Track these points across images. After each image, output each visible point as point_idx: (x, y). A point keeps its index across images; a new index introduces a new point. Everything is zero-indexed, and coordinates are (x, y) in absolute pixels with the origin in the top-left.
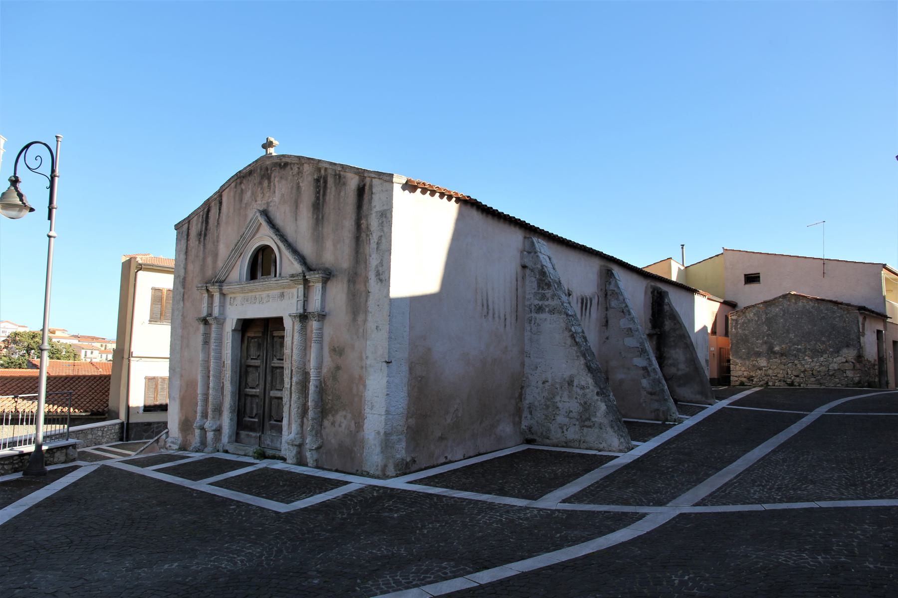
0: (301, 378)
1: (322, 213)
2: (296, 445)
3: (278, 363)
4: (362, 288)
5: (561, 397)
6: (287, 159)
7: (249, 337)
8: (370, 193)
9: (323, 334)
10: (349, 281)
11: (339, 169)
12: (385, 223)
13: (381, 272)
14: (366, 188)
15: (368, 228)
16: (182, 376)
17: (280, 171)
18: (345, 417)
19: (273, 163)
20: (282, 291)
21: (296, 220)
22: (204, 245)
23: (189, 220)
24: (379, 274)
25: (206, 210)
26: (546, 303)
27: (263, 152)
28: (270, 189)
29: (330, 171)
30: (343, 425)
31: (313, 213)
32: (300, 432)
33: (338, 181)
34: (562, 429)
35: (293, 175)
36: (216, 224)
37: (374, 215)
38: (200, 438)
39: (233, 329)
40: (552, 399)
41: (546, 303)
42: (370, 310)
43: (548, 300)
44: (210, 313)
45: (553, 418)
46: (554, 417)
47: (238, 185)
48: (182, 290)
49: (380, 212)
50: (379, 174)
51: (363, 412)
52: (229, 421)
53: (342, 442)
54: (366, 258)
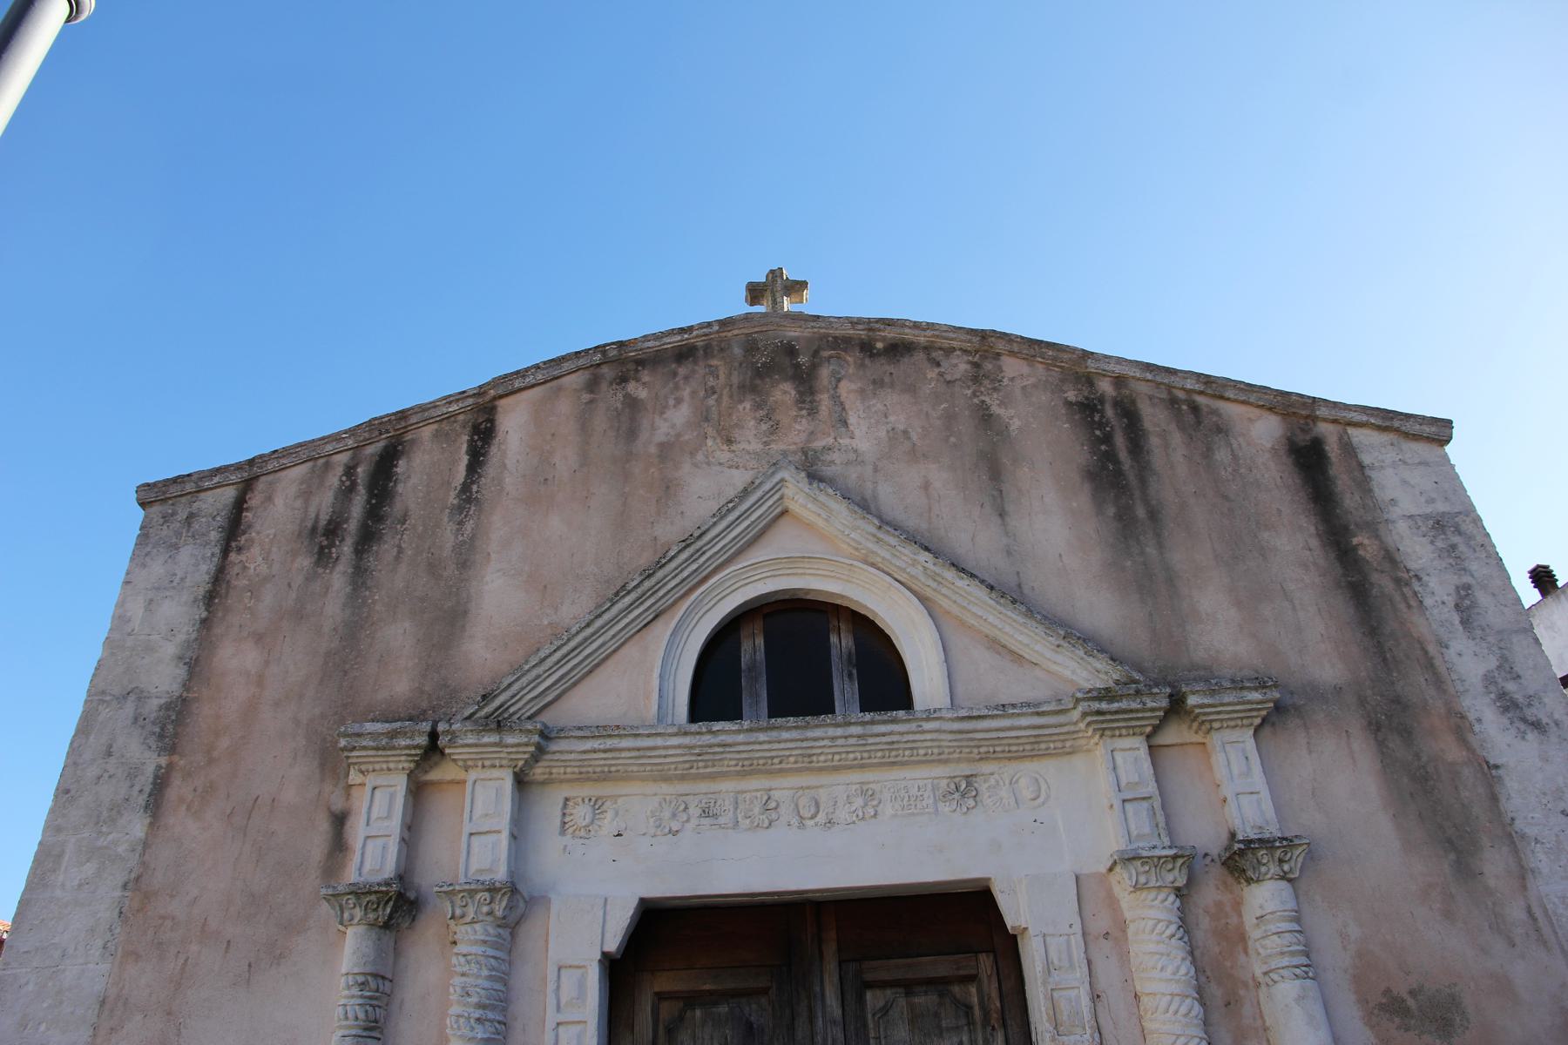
1: (1146, 501)
6: (907, 331)
7: (660, 997)
12: (1462, 548)
13: (1519, 697)
17: (867, 361)
19: (828, 335)
20: (966, 769)
21: (1002, 514)
22: (360, 575)
25: (373, 450)
28: (813, 412)
31: (1099, 505)
33: (1190, 418)
36: (452, 499)
37: (1402, 527)
39: (613, 945)
47: (604, 386)
48: (151, 761)
49: (1426, 517)
50: (1389, 422)
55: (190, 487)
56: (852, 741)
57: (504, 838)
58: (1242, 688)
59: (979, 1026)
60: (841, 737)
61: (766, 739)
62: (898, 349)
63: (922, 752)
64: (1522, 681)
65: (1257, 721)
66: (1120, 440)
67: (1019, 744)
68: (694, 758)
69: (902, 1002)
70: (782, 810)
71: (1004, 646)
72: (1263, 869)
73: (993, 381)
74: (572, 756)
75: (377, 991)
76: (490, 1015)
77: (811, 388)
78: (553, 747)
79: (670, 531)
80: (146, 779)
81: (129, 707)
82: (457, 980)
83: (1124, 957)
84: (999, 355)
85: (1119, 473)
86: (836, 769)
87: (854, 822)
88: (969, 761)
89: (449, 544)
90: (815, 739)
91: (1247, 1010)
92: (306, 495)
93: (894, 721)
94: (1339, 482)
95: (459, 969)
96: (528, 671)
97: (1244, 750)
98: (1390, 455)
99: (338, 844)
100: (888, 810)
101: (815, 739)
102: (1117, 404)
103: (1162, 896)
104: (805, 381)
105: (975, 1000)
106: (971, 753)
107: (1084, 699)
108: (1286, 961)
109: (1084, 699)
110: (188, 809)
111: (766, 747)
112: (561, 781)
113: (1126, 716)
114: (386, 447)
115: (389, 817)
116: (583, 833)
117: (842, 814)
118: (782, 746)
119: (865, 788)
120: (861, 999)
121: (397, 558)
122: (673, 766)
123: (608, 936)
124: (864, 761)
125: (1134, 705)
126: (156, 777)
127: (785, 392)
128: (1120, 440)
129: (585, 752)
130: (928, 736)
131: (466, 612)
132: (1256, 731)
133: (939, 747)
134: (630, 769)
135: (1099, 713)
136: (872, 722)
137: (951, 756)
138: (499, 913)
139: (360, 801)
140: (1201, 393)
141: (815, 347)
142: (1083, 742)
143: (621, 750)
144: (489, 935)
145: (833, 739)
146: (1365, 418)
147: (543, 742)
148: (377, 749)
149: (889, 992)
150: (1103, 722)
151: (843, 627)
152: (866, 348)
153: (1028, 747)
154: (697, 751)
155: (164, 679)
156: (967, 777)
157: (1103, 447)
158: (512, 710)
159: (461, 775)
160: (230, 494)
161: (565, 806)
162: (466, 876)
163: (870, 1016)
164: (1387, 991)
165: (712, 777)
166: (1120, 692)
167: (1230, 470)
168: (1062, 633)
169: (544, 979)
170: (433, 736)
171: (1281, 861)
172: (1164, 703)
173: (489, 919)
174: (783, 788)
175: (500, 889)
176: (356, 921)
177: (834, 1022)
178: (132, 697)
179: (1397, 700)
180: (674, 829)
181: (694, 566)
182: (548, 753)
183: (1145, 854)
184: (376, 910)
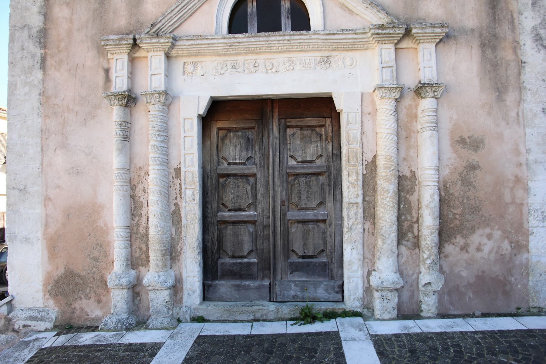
2: (397, 290)
3: (303, 168)
4: (509, 55)
7: (219, 129)
10: (483, 45)
16: (47, 199)
18: (489, 237)
20: (327, 54)
24: (541, 39)
30: (486, 249)
38: (127, 304)
42: (528, 87)
44: (130, 88)
48: (39, 52)
51: (525, 226)
53: (483, 272)
54: (512, 16)
56: (286, 42)
57: (163, 76)
58: (434, 27)
59: (324, 141)
60: (282, 40)
61: (254, 40)
63: (311, 47)
65: (438, 40)
67: (347, 45)
68: (228, 47)
69: (299, 132)
70: (260, 67)
71: (346, 7)
72: (427, 94)
74: (185, 47)
75: (126, 126)
76: (162, 134)
78: (178, 43)
82: (151, 123)
83: (374, 121)
86: (280, 52)
87: (285, 72)
88: (329, 51)
90: (272, 41)
91: (413, 140)
93: (301, 35)
95: (151, 119)
96: (167, 15)
99: (108, 80)
100: (298, 67)
101: (272, 41)
103: (390, 101)
105: (323, 133)
106: (329, 47)
107: (373, 28)
108: (429, 125)
109: (373, 28)
110: (55, 68)
111: (254, 43)
112: (182, 56)
113: (388, 36)
115: (123, 69)
116: (191, 75)
117: (281, 68)
118: (260, 43)
119: (290, 59)
120: (285, 131)
122: (221, 50)
123: (200, 109)
124: (290, 50)
125: (392, 32)
126: (42, 57)
129: (189, 45)
130: (314, 41)
132: (437, 44)
133: (318, 45)
134: (206, 51)
135: (378, 34)
136: (293, 35)
137: (322, 49)
138: (162, 101)
139: (113, 64)
142: (371, 45)
143: (202, 44)
144: (160, 108)
145: (279, 41)
148: (115, 45)
149: (295, 129)
150: (379, 38)
153: (350, 46)
154: (229, 45)
156: (327, 56)
158: (163, 30)
159: (147, 54)
161: (184, 65)
162: (151, 88)
163: (288, 136)
164: (461, 136)
165: (236, 55)
166: (387, 26)
168: (369, 2)
169: (179, 123)
170: (135, 40)
171: (434, 91)
172: (403, 31)
173: (159, 103)
174: (261, 59)
175: (162, 93)
176: (116, 104)
177: (276, 138)
178: (26, 28)
179: (494, 35)
180: (222, 73)
182: (176, 46)
183: (386, 86)
184: (121, 101)
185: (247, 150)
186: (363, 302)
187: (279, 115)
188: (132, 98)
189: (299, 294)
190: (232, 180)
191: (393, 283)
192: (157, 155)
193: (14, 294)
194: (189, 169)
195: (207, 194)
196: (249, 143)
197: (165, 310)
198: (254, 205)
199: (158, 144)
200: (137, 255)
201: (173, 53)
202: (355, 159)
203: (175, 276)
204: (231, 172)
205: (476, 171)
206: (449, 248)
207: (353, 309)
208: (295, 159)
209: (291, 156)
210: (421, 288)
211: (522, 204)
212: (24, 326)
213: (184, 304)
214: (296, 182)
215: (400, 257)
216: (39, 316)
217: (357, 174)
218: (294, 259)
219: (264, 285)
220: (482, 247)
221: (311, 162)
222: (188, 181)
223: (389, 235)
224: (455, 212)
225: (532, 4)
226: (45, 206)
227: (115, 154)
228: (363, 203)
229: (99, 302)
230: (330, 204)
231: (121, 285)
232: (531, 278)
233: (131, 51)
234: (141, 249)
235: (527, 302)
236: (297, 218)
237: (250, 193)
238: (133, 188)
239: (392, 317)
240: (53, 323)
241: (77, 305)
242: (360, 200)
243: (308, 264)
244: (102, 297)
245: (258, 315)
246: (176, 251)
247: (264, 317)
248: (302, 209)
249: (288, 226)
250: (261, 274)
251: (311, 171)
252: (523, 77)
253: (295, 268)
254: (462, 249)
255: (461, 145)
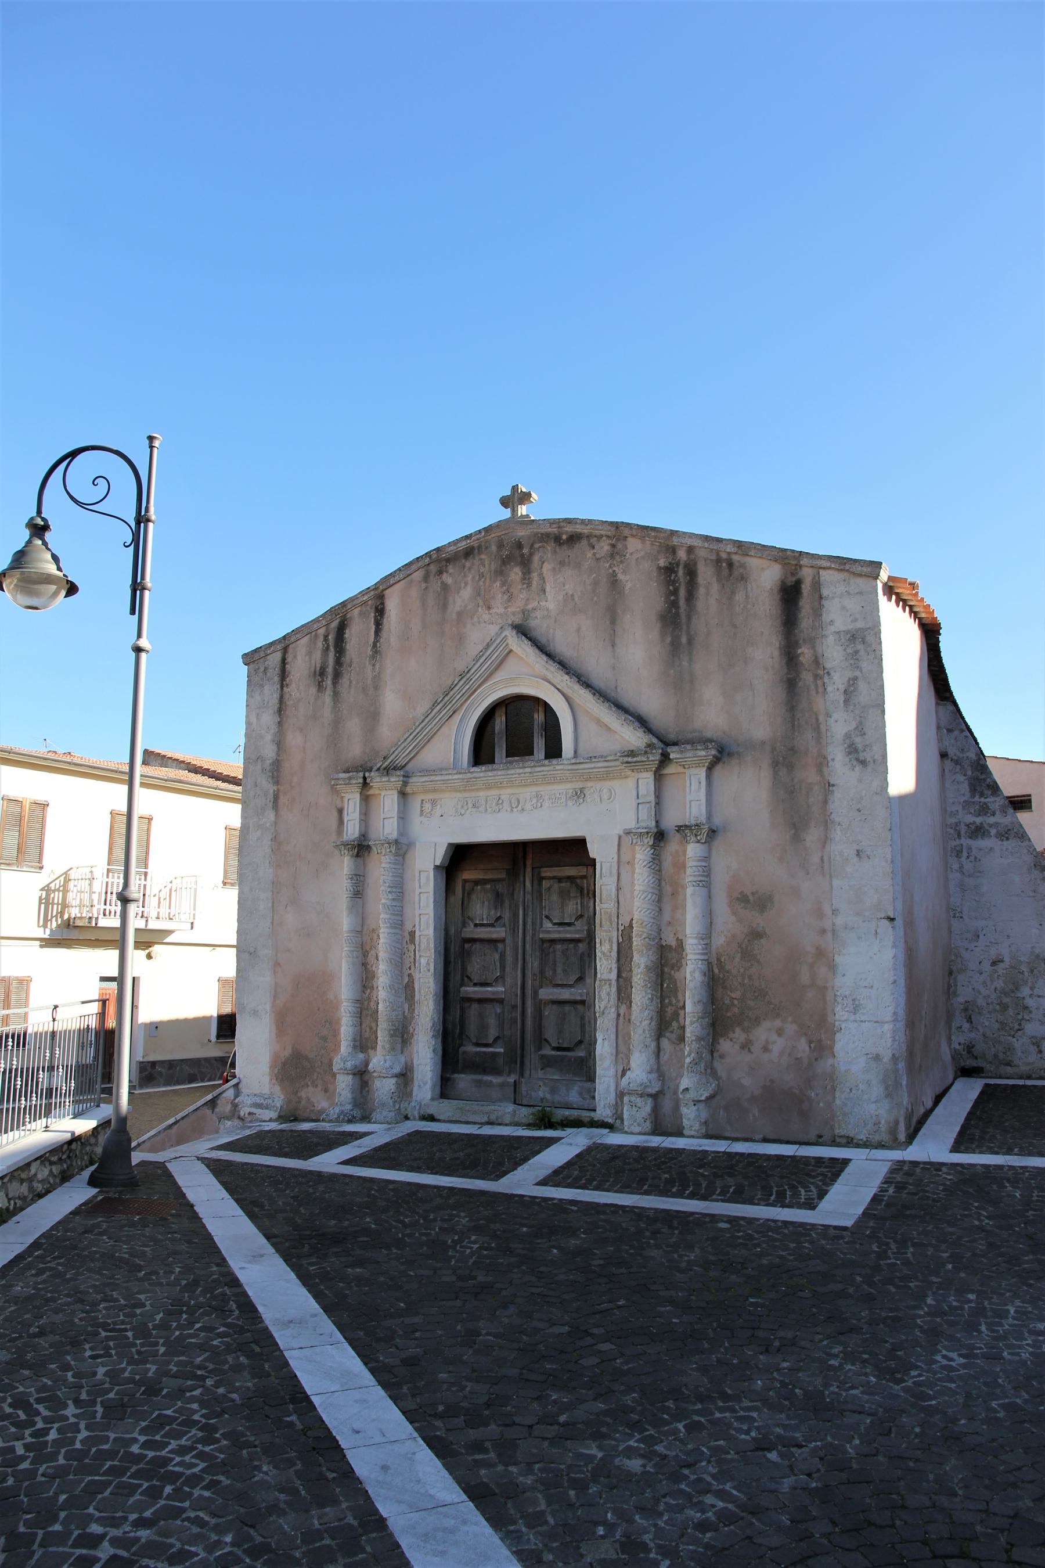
0: (653, 958)
1: (688, 633)
2: (650, 1095)
3: (559, 932)
4: (811, 776)
5: (1032, 989)
6: (578, 526)
7: (465, 881)
8: (817, 596)
9: (710, 870)
10: (775, 764)
11: (730, 548)
12: (862, 653)
13: (860, 747)
14: (803, 586)
15: (817, 662)
16: (277, 964)
17: (557, 549)
18: (780, 1032)
19: (537, 533)
20: (580, 785)
21: (613, 645)
22: (336, 694)
23: (285, 645)
24: (856, 751)
25: (334, 624)
26: (992, 820)
27: (506, 514)
28: (529, 585)
29: (702, 554)
30: (776, 1049)
31: (663, 635)
32: (656, 1067)
33: (726, 572)
34: (1038, 1046)
35: (598, 559)
36: (370, 653)
37: (831, 639)
38: (352, 1093)
39: (438, 863)
40: (1013, 992)
41: (992, 820)
42: (837, 820)
43: (994, 814)
44: (363, 833)
45: (1017, 1027)
46: (1020, 1025)
47: (432, 577)
48: (272, 788)
49: (846, 632)
50: (843, 564)
51: (830, 1019)
52: (432, 1054)
53: (772, 1081)
54: (817, 720)
55: (262, 654)
56: (527, 775)
58: (696, 750)
62: (574, 539)
64: (866, 737)
66: (682, 592)
69: (556, 886)
70: (504, 804)
73: (620, 557)
76: (394, 890)
77: (529, 569)
78: (411, 780)
79: (460, 665)
80: (271, 796)
81: (259, 766)
84: (626, 537)
85: (677, 615)
89: (370, 678)
92: (310, 653)
93: (543, 765)
94: (803, 611)
97: (699, 779)
98: (841, 589)
99: (341, 821)
100: (546, 804)
102: (687, 566)
104: (525, 563)
108: (691, 878)
114: (340, 622)
117: (528, 806)
120: (540, 884)
121: (350, 686)
125: (644, 759)
127: (516, 574)
128: (682, 592)
131: (379, 713)
132: (710, 769)
135: (627, 762)
136: (535, 766)
140: (736, 553)
141: (531, 542)
145: (519, 774)
146: (828, 564)
147: (405, 779)
151: (540, 709)
152: (557, 539)
155: (269, 751)
157: (672, 598)
160: (278, 655)
161: (422, 803)
164: (742, 892)
165: (477, 790)
167: (742, 606)
170: (365, 778)
171: (696, 835)
172: (658, 757)
174: (505, 793)
181: (468, 687)
185: (496, 908)
186: (617, 1111)
187: (532, 863)
188: (364, 846)
189: (548, 1096)
190: (478, 946)
191: (641, 1085)
192: (388, 916)
193: (242, 1077)
194: (425, 933)
195: (450, 963)
196: (498, 899)
197: (391, 1102)
198: (500, 979)
199: (388, 902)
200: (367, 1035)
201: (408, 790)
202: (608, 923)
203: (406, 1063)
204: (476, 936)
205: (762, 940)
206: (725, 1045)
207: (602, 1118)
208: (551, 920)
209: (547, 917)
210: (681, 1096)
211: (825, 988)
212: (250, 1114)
213: (414, 1098)
214: (551, 949)
215: (662, 1053)
216: (265, 1103)
217: (610, 941)
218: (547, 1051)
219: (508, 1082)
220: (770, 1047)
221: (569, 924)
222: (422, 947)
223: (641, 1022)
224: (733, 995)
225: (844, 701)
226: (274, 973)
227: (345, 913)
228: (618, 980)
229: (326, 1091)
230: (589, 981)
231: (346, 1069)
232: (837, 1094)
233: (362, 789)
234: (371, 1028)
235: (832, 1128)
236: (551, 997)
237: (498, 964)
238: (365, 954)
239: (643, 1132)
240: (277, 1113)
241: (303, 1094)
242: (613, 976)
243: (562, 1059)
244: (329, 1086)
245: (493, 1117)
246: (408, 1033)
247: (500, 1121)
248: (558, 985)
249: (540, 1008)
250: (507, 1068)
251: (568, 936)
252: (832, 806)
253: (547, 1063)
254: (743, 1047)
255: (742, 905)
